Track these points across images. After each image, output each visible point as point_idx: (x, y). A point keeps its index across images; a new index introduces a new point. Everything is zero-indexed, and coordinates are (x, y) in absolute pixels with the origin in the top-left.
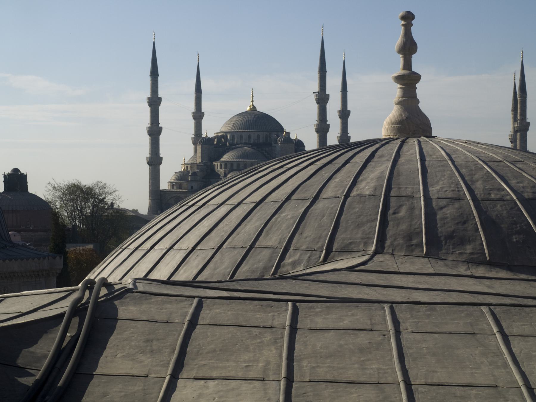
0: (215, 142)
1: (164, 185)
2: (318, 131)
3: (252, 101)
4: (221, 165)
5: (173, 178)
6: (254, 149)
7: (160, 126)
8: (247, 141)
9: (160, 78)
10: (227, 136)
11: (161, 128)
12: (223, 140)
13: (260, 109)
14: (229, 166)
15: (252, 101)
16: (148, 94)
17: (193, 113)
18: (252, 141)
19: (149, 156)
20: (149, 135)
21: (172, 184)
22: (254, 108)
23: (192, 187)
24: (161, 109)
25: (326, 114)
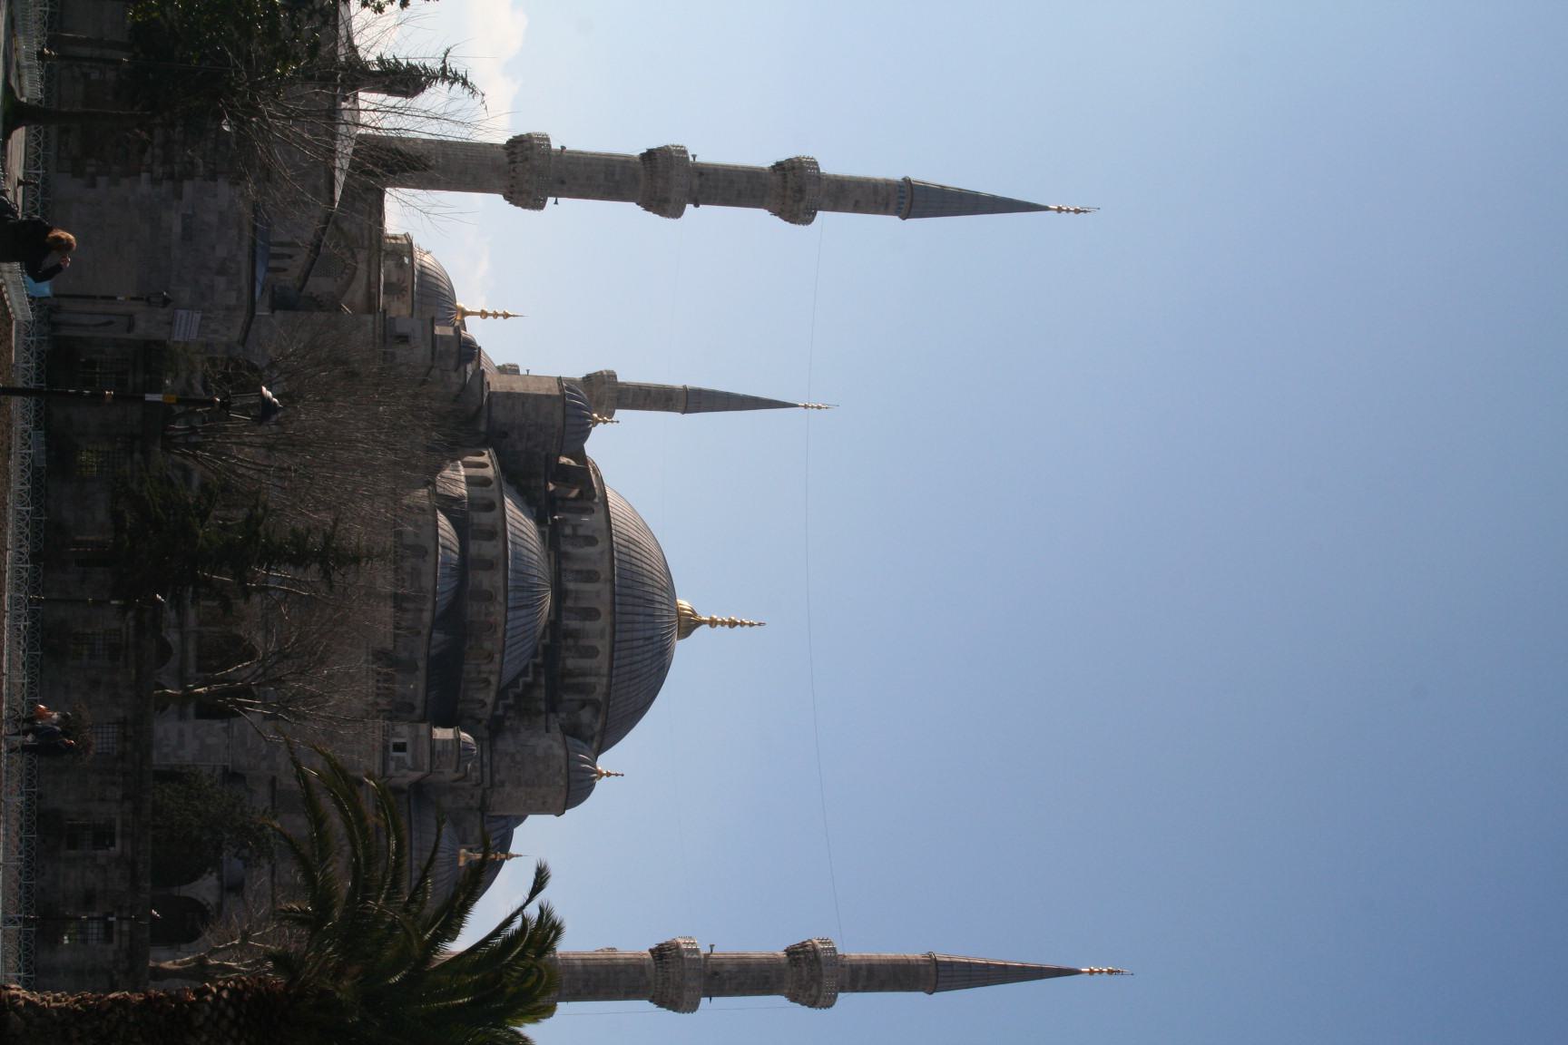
0: (564, 460)
1: (406, 212)
2: (664, 954)
3: (713, 623)
4: (485, 482)
5: (427, 260)
6: (543, 636)
7: (689, 207)
8: (570, 603)
9: (891, 222)
10: (590, 511)
11: (677, 213)
12: (574, 493)
13: (684, 651)
14: (485, 518)
15: (713, 623)
16: (833, 164)
17: (612, 376)
18: (574, 624)
19: (555, 145)
20: (650, 155)
21: (403, 250)
22: (689, 624)
23: (404, 339)
24: (759, 219)
25: (744, 994)
